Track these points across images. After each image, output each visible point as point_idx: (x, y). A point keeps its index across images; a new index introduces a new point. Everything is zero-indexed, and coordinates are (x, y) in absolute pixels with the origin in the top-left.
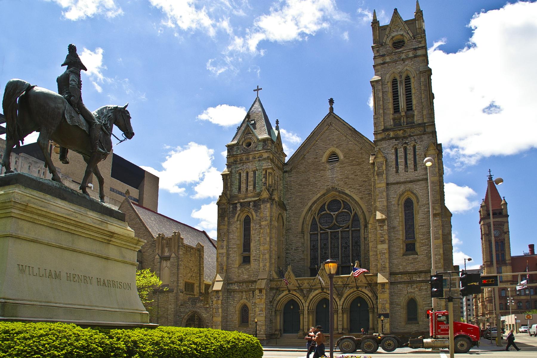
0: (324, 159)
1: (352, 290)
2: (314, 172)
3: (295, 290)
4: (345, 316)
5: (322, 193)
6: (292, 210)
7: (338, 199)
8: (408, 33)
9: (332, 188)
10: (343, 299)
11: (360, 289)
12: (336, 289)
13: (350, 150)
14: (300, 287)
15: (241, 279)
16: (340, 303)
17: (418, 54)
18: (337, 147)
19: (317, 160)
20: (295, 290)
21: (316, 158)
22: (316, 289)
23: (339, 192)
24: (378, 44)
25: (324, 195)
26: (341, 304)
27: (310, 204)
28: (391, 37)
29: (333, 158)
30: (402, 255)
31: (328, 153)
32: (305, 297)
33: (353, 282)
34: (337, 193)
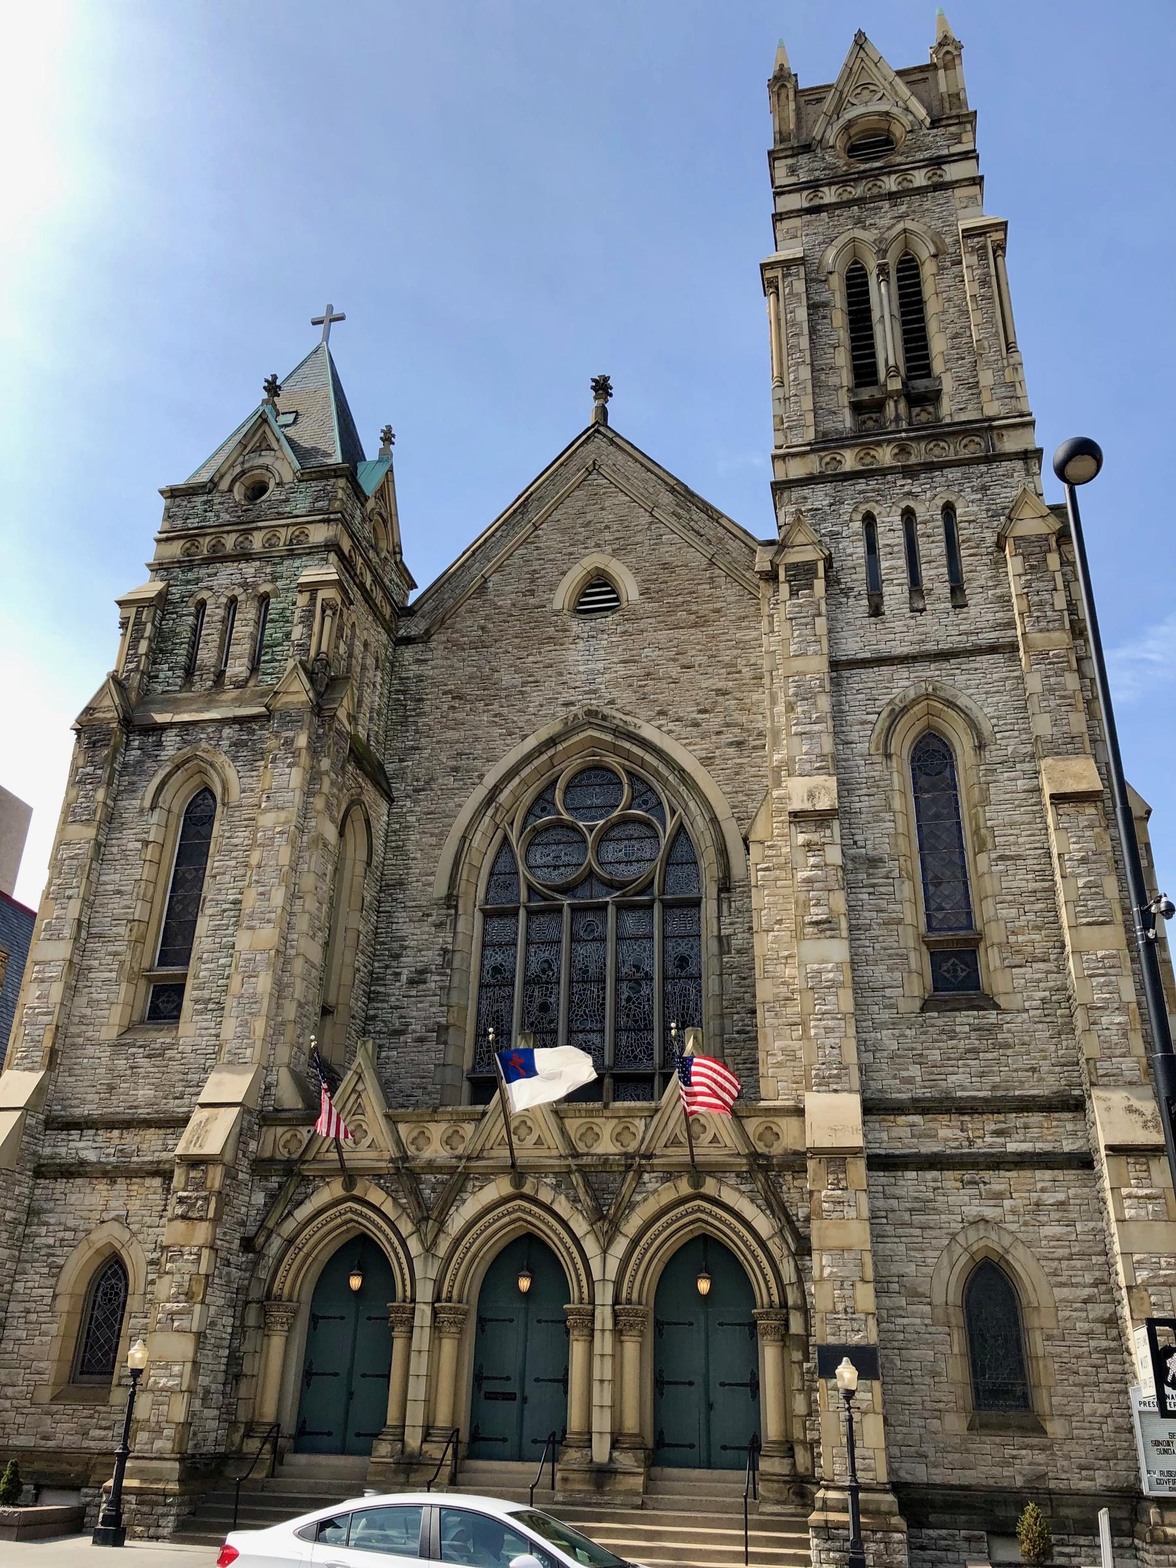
0: (563, 596)
1: (667, 1194)
2: (517, 647)
3: (377, 1176)
4: (631, 1349)
5: (544, 734)
6: (416, 802)
7: (612, 760)
8: (907, 109)
9: (589, 713)
10: (620, 1247)
11: (710, 1186)
12: (587, 1184)
13: (665, 566)
14: (405, 1158)
15: (117, 1107)
16: (605, 1265)
17: (947, 178)
18: (615, 553)
19: (532, 601)
20: (377, 1176)
21: (532, 593)
22: (487, 1176)
23: (617, 732)
24: (792, 146)
25: (552, 742)
26: (612, 1274)
27: (490, 780)
28: (842, 122)
29: (598, 596)
30: (918, 1004)
31: (575, 575)
32: (430, 1217)
33: (674, 1142)
34: (609, 738)
